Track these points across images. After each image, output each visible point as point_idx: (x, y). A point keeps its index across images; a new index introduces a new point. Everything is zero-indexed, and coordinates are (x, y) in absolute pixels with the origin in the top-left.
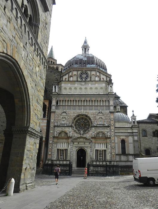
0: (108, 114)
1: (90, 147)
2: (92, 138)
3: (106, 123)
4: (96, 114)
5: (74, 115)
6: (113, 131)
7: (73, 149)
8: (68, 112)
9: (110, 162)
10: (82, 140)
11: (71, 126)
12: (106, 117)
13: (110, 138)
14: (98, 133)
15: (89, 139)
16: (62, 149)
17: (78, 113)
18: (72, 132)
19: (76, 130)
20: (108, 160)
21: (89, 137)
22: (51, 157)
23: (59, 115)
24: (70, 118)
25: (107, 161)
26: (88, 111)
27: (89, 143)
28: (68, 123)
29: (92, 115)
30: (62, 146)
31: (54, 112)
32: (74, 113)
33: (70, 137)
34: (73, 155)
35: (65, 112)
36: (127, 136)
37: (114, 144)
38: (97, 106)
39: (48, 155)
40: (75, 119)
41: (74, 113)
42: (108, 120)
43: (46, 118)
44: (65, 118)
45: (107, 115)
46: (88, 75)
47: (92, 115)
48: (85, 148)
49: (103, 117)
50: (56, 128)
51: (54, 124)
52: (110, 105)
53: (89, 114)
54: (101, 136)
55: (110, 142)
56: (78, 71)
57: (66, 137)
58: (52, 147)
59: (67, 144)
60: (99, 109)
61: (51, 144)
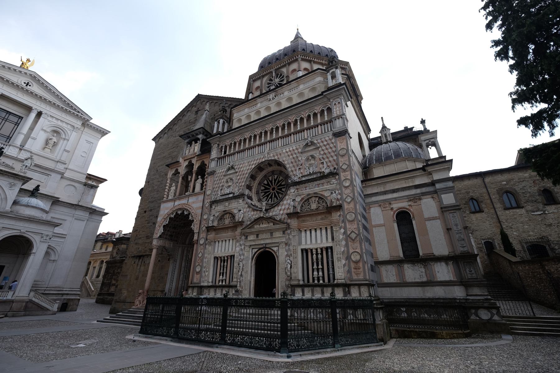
0: (329, 142)
1: (286, 244)
2: (290, 215)
4: (299, 152)
6: (347, 184)
7: (243, 255)
9: (346, 287)
10: (264, 226)
11: (241, 196)
12: (326, 151)
13: (339, 207)
14: (307, 200)
15: (281, 222)
16: (224, 257)
17: (258, 161)
18: (245, 210)
19: (258, 204)
20: (340, 281)
21: (282, 215)
22: (199, 279)
24: (241, 177)
25: (338, 285)
28: (236, 189)
29: (289, 156)
30: (223, 249)
31: (213, 173)
32: (250, 163)
34: (245, 270)
35: (232, 168)
36: (416, 199)
37: (355, 226)
38: (302, 131)
39: (195, 275)
40: (253, 177)
42: (332, 157)
45: (328, 144)
46: (283, 77)
48: (273, 248)
49: (316, 154)
50: (213, 207)
52: (335, 115)
53: (283, 155)
54: (314, 206)
55: (343, 221)
56: (263, 76)
58: (203, 255)
59: (234, 241)
61: (202, 246)
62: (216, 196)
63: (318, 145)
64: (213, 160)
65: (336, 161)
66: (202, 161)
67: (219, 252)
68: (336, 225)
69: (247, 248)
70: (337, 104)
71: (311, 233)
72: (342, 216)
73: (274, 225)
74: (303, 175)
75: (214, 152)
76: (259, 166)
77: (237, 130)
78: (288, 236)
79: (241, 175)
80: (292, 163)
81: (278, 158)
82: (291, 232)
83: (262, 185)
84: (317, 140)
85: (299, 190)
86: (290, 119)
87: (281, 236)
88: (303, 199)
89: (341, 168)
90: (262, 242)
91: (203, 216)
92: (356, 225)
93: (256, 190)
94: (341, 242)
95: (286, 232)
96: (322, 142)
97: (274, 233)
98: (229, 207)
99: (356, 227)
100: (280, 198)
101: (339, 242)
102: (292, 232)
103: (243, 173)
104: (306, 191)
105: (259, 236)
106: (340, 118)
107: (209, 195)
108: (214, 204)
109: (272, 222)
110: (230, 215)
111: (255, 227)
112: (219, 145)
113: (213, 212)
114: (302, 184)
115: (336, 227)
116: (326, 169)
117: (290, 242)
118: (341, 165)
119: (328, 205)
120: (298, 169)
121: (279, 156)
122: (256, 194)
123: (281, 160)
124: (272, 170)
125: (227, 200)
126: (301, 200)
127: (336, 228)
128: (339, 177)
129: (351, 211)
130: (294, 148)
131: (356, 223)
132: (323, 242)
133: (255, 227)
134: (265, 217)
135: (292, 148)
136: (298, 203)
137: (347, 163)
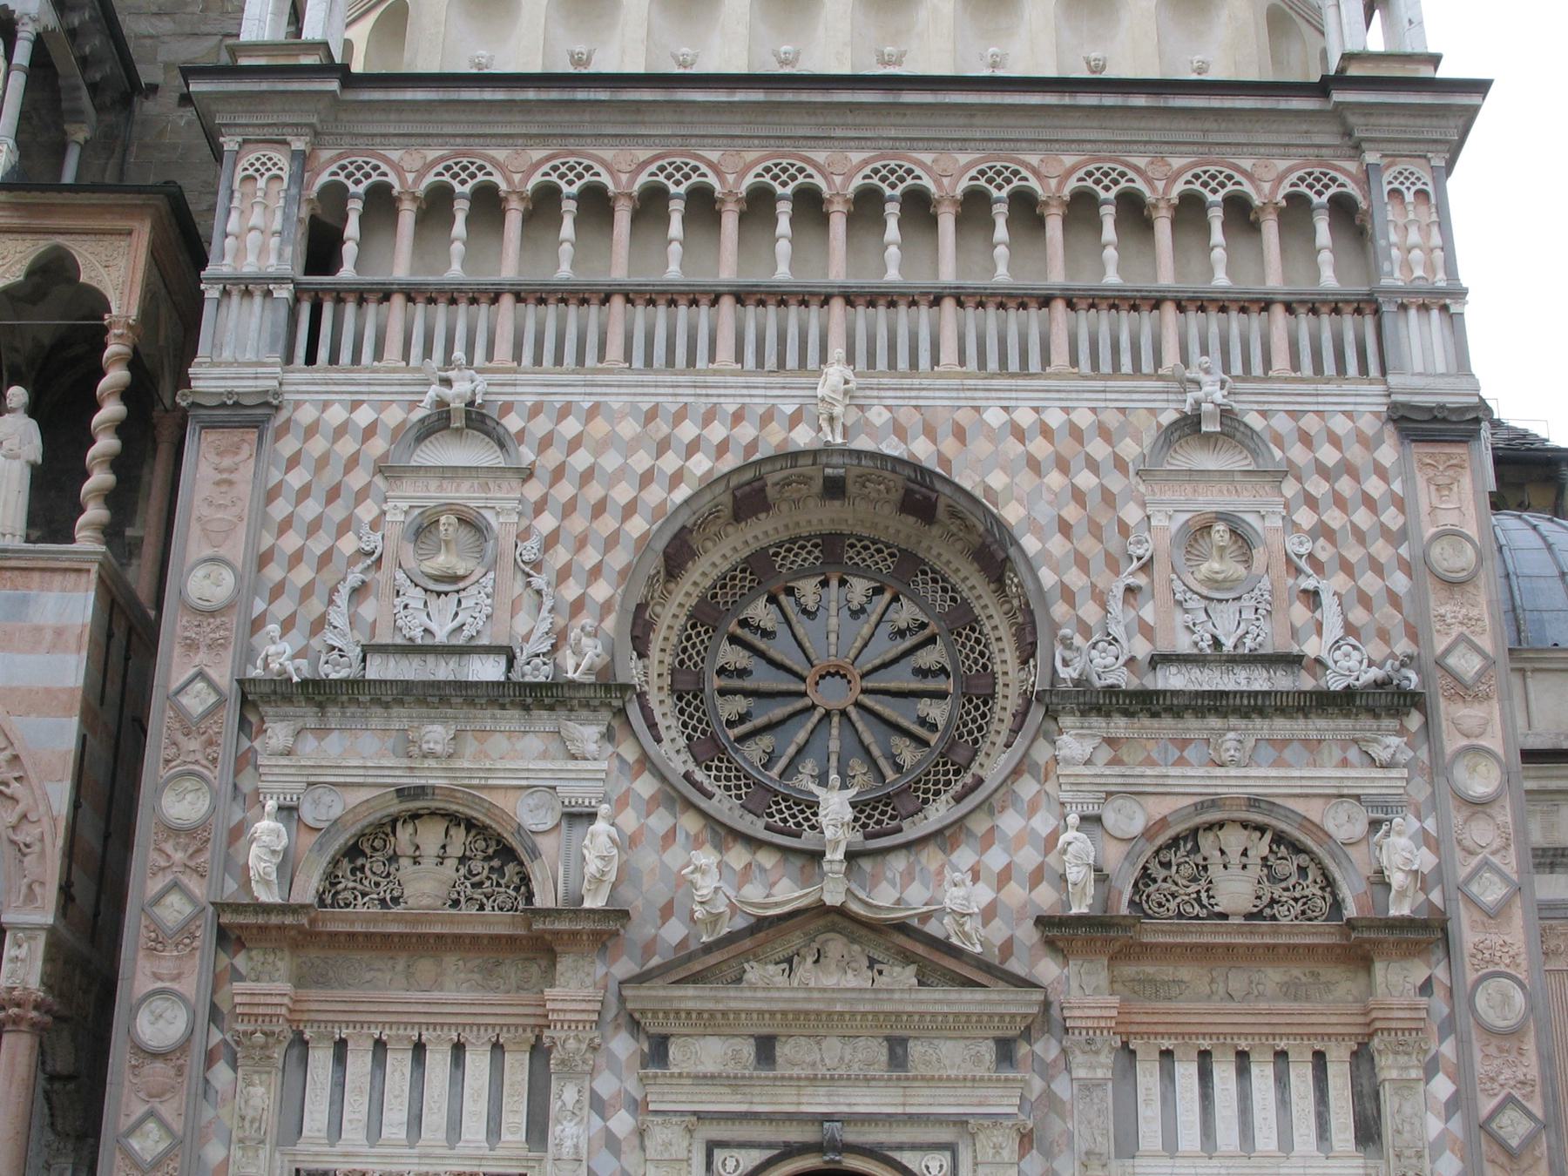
0: (1356, 453)
1: (1026, 1140)
3: (1333, 628)
4: (1120, 464)
5: (670, 462)
8: (535, 411)
12: (1334, 518)
15: (991, 971)
17: (747, 432)
18: (629, 820)
21: (989, 913)
23: (358, 479)
24: (578, 523)
26: (940, 397)
27: (1005, 1051)
29: (1034, 465)
32: (661, 428)
33: (574, 910)
35: (478, 420)
37: (1530, 1067)
41: (661, 428)
42: (1377, 568)
43: (86, 541)
44: (471, 523)
47: (1034, 465)
50: (278, 733)
51: (249, 655)
53: (980, 447)
55: (1449, 1026)
57: (497, 921)
59: (517, 1067)
60: (1171, 357)
61: (159, 1071)
62: (297, 638)
63: (1278, 454)
64: (247, 286)
65: (1406, 605)
66: (42, 244)
67: (354, 1132)
68: (1405, 1043)
69: (664, 1137)
70: (1409, 197)
71: (1205, 1076)
72: (1439, 993)
73: (921, 983)
74: (1163, 647)
75: (256, 218)
76: (761, 478)
77: (531, 95)
78: (1037, 1084)
79: (569, 508)
80: (1065, 528)
81: (944, 460)
82: (1064, 1051)
83: (733, 627)
84: (1263, 414)
85: (1124, 753)
86: (1035, 172)
87: (980, 1072)
88: (1163, 823)
89: (1439, 663)
90: (817, 1102)
91: (158, 792)
92: (1532, 1058)
93: (668, 659)
94: (1433, 1161)
95: (1023, 1049)
96: (1306, 439)
97: (916, 1049)
98: (458, 764)
99: (1533, 1072)
100: (898, 768)
101: (1419, 1155)
102: (1078, 1058)
103: (595, 492)
104: (1190, 772)
105: (783, 1051)
106: (1435, 313)
107: (212, 613)
108: (290, 710)
109: (907, 958)
110: (459, 834)
111: (754, 973)
112: (303, 161)
113: (277, 785)
114: (1155, 715)
115: (1402, 1059)
116: (1336, 645)
117: (1057, 1126)
118: (1441, 645)
119: (1337, 905)
120: (1119, 591)
121: (949, 445)
122: (673, 690)
123: (967, 485)
124: (827, 528)
125: (444, 701)
126: (1148, 833)
127: (1406, 1068)
128: (1426, 722)
129: (1502, 968)
130: (1083, 419)
131: (1530, 1045)
132: (1299, 1147)
133: (754, 973)
134: (855, 907)
135: (1066, 410)
136: (1123, 848)
137: (1486, 643)
